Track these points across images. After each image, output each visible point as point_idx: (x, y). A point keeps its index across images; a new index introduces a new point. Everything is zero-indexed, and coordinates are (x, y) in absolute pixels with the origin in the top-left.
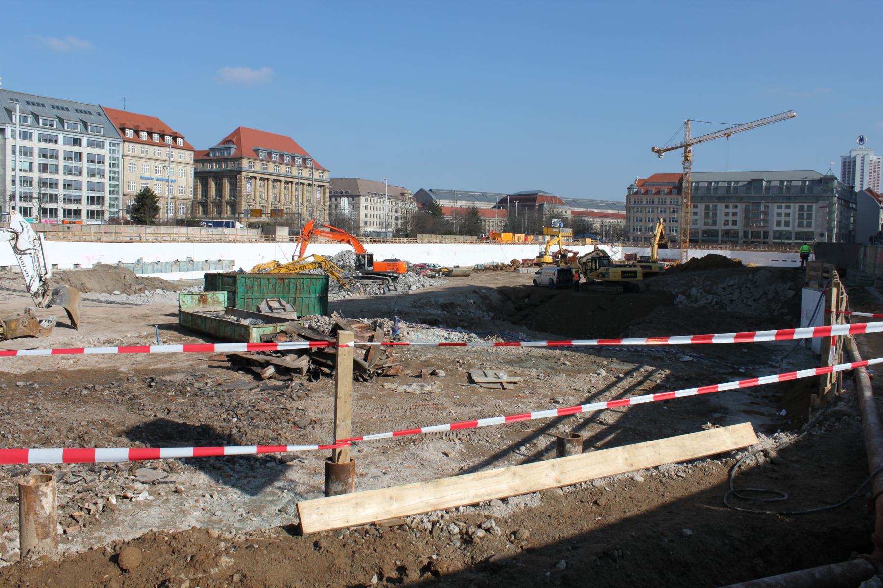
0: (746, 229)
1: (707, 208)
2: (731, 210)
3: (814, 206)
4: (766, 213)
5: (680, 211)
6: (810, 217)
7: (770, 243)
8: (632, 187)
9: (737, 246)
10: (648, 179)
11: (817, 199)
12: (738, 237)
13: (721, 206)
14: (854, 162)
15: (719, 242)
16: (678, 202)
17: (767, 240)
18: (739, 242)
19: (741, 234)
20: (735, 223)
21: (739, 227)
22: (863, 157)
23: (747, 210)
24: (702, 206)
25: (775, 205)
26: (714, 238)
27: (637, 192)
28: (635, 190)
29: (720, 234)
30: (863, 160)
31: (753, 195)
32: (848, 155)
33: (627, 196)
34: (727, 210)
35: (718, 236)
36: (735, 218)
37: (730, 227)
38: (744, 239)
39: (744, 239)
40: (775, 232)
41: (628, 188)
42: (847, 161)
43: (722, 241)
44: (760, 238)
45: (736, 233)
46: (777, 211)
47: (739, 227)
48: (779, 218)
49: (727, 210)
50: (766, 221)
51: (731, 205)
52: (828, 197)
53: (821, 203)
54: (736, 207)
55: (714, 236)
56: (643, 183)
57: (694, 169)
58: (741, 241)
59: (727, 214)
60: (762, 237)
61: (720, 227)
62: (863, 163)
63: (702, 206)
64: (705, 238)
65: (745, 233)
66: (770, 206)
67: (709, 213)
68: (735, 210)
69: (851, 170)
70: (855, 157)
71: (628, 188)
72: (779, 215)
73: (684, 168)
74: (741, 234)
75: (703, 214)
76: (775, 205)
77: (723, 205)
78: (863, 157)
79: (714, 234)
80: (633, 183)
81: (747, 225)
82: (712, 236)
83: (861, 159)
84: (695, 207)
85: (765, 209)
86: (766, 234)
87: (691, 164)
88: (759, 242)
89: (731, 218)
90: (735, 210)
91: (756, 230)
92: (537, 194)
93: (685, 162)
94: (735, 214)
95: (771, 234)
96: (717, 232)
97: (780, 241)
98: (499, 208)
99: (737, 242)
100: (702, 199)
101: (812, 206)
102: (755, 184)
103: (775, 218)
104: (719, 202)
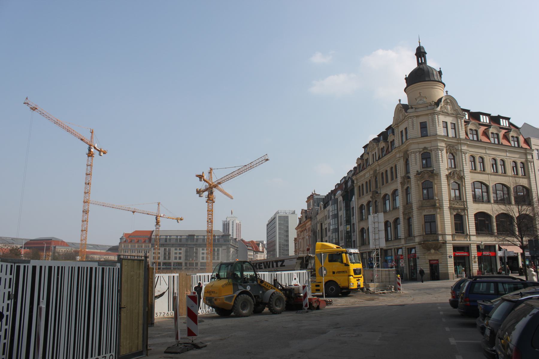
0: (186, 261)
1: (165, 249)
2: (178, 251)
3: (220, 249)
4: (196, 253)
5: (150, 252)
6: (218, 254)
7: (199, 269)
8: (123, 238)
9: (182, 271)
10: (132, 233)
11: (221, 245)
12: (182, 266)
13: (173, 250)
14: (229, 224)
15: (172, 269)
16: (149, 247)
17: (197, 267)
18: (183, 269)
19: (183, 264)
20: (180, 258)
21: (182, 261)
22: (233, 221)
23: (186, 252)
24: (162, 249)
25: (201, 249)
26: (169, 267)
27: (125, 241)
28: (124, 240)
29: (172, 264)
30: (233, 223)
31: (190, 243)
32: (225, 220)
33: (119, 243)
34: (176, 251)
35: (171, 266)
36: (180, 256)
37: (178, 261)
38: (185, 267)
39: (185, 267)
40: (201, 263)
41: (120, 239)
42: (225, 223)
43: (174, 269)
44: (193, 266)
45: (180, 264)
46: (201, 251)
47: (182, 261)
48: (203, 256)
49: (176, 251)
50: (196, 257)
51: (178, 249)
52: (227, 244)
53: (224, 247)
54: (180, 249)
55: (169, 266)
56: (128, 236)
57: (161, 229)
58: (183, 268)
59: (176, 253)
60: (195, 266)
61: (172, 260)
62: (233, 224)
63: (162, 249)
64: (164, 267)
65: (186, 264)
66: (198, 249)
67: (166, 254)
68: (180, 251)
69: (228, 227)
70: (229, 221)
71: (120, 239)
72: (203, 253)
73: (156, 228)
74: (183, 264)
75: (163, 254)
76: (201, 249)
77: (174, 248)
78: (233, 221)
79: (169, 264)
80: (122, 236)
81: (186, 259)
82: (168, 266)
83: (232, 222)
84: (159, 249)
85: (196, 251)
86: (197, 264)
87: (159, 226)
88: (193, 268)
89: (178, 255)
90: (180, 251)
91: (192, 262)
92: (52, 239)
93: (156, 225)
94: (180, 253)
95: (199, 264)
96: (171, 263)
97: (204, 267)
98: (24, 248)
99: (182, 269)
100: (162, 245)
101: (219, 249)
102: (191, 236)
103: (201, 256)
104: (172, 247)
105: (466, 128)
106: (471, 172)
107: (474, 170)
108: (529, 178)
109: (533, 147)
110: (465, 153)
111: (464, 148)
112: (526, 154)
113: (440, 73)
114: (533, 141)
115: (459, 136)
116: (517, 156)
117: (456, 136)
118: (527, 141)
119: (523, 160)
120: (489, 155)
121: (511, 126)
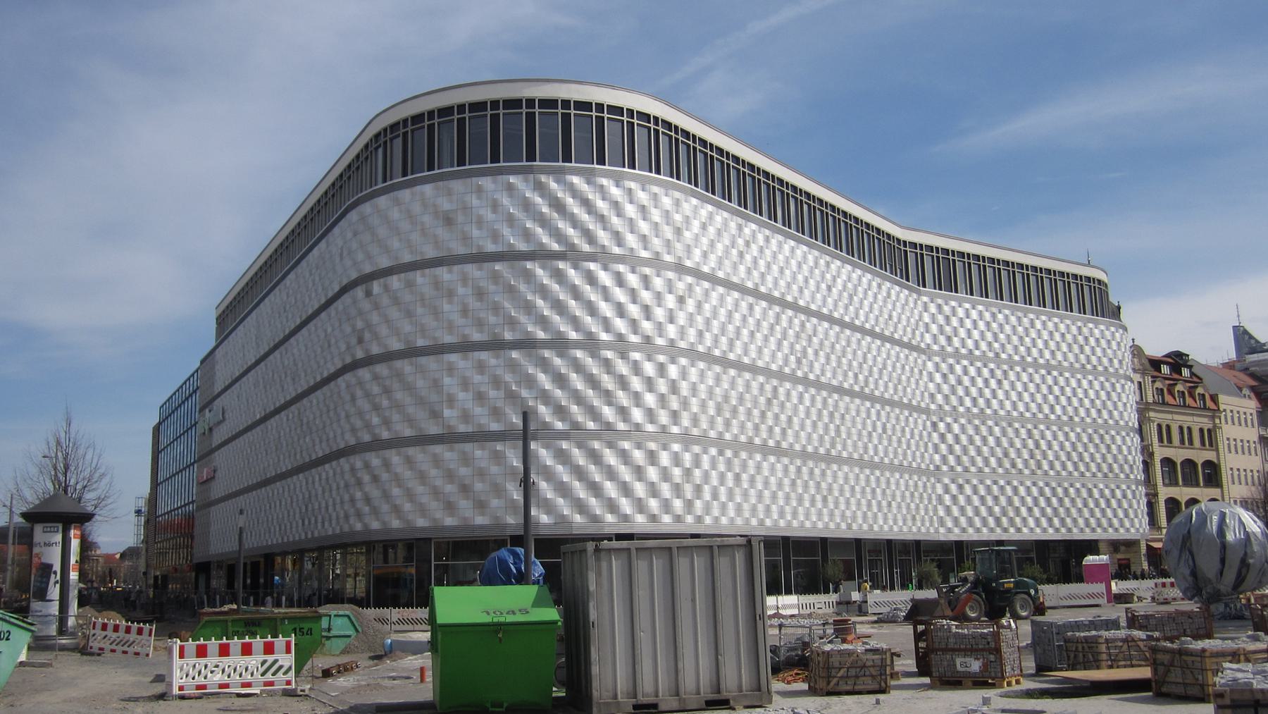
105: (1152, 386)
106: (1160, 446)
107: (1161, 440)
108: (1217, 450)
109: (1222, 407)
110: (1153, 422)
111: (1152, 414)
112: (1213, 418)
113: (1119, 308)
114: (1222, 398)
115: (1146, 398)
116: (1205, 420)
117: (1142, 399)
118: (1214, 398)
119: (1210, 426)
120: (1177, 420)
121: (1194, 377)
